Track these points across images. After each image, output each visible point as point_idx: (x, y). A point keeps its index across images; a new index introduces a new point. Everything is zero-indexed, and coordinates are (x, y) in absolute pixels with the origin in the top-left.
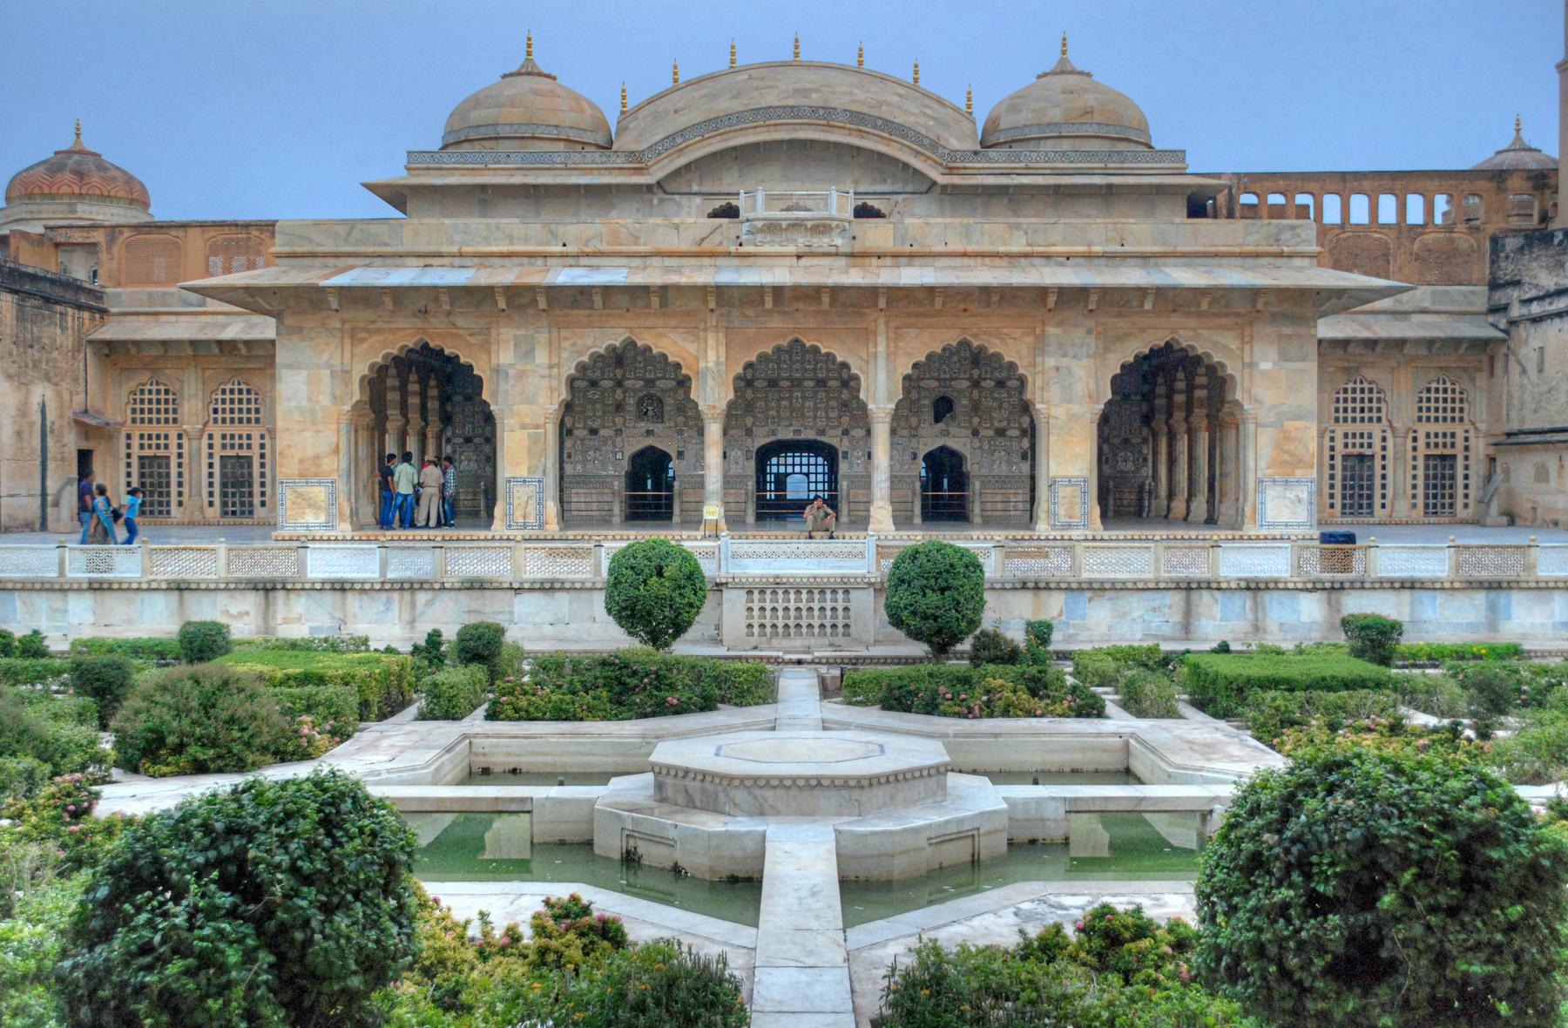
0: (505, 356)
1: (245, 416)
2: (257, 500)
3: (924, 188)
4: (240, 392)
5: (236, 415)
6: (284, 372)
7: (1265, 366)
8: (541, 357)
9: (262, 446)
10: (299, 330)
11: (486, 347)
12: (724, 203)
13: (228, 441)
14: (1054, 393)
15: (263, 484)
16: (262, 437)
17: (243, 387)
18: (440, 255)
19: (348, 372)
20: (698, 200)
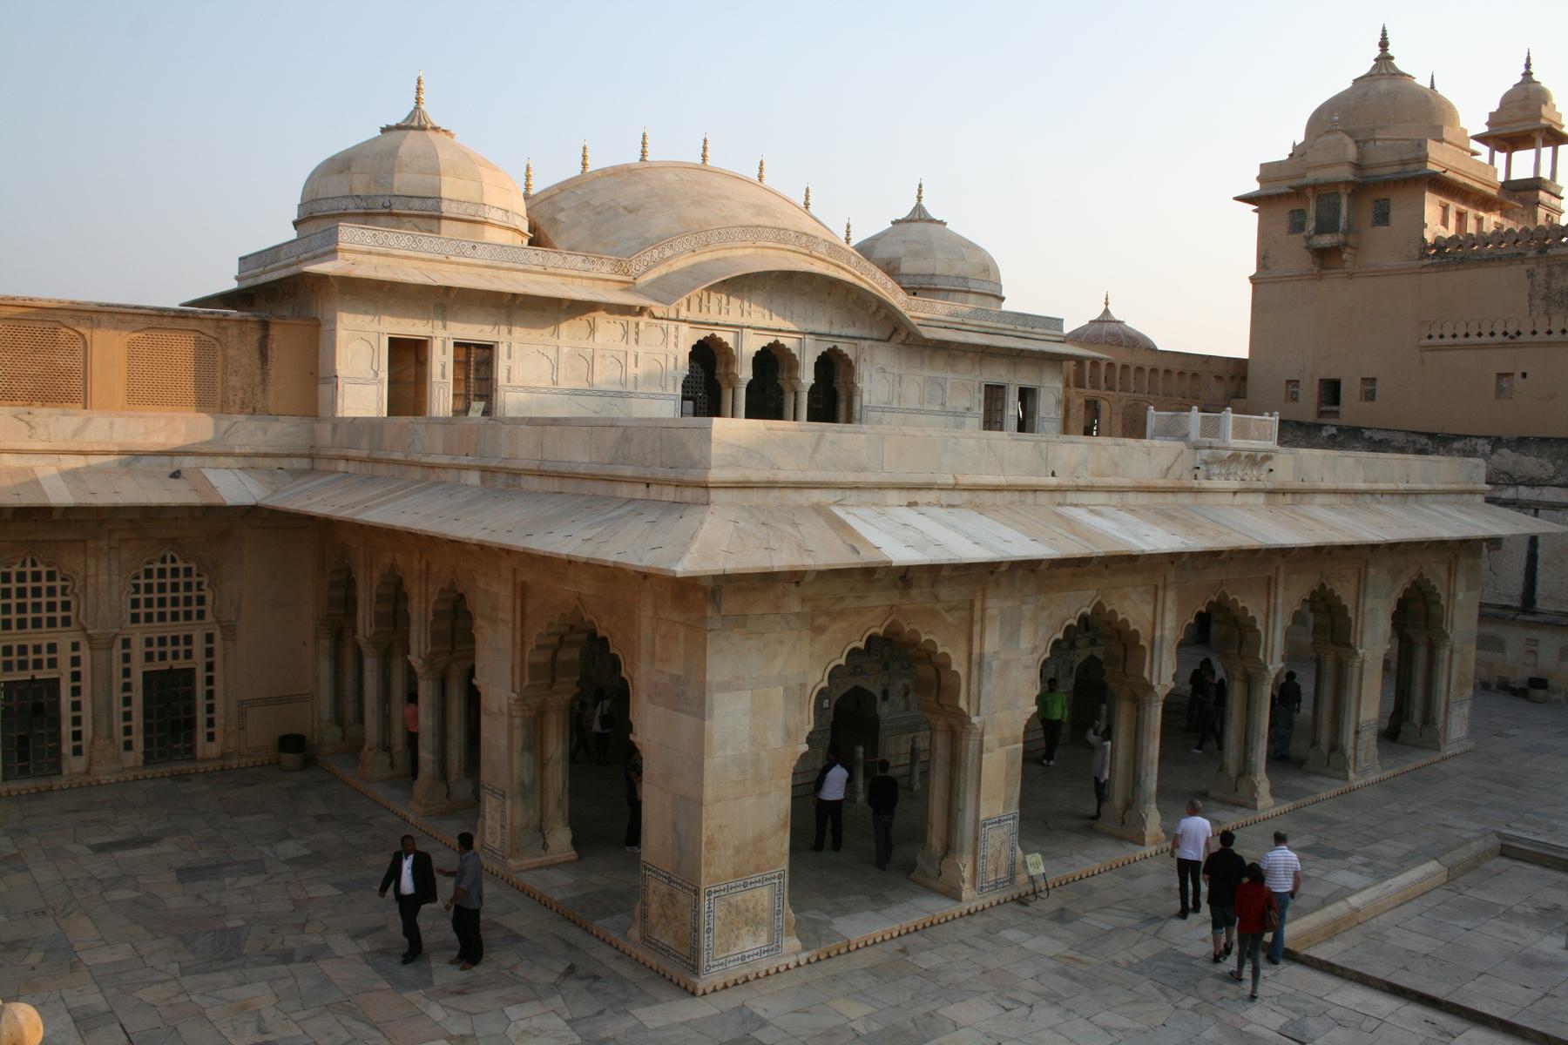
0: (992, 642)
1: (44, 615)
2: (67, 747)
3: (886, 336)
4: (37, 577)
5: (29, 615)
6: (717, 696)
7: (1460, 596)
8: (1026, 640)
9: (76, 661)
10: (741, 620)
11: (969, 629)
12: (708, 333)
13: (15, 657)
14: (1367, 639)
15: (77, 721)
16: (75, 646)
17: (43, 569)
18: (929, 487)
19: (803, 686)
20: (685, 328)
